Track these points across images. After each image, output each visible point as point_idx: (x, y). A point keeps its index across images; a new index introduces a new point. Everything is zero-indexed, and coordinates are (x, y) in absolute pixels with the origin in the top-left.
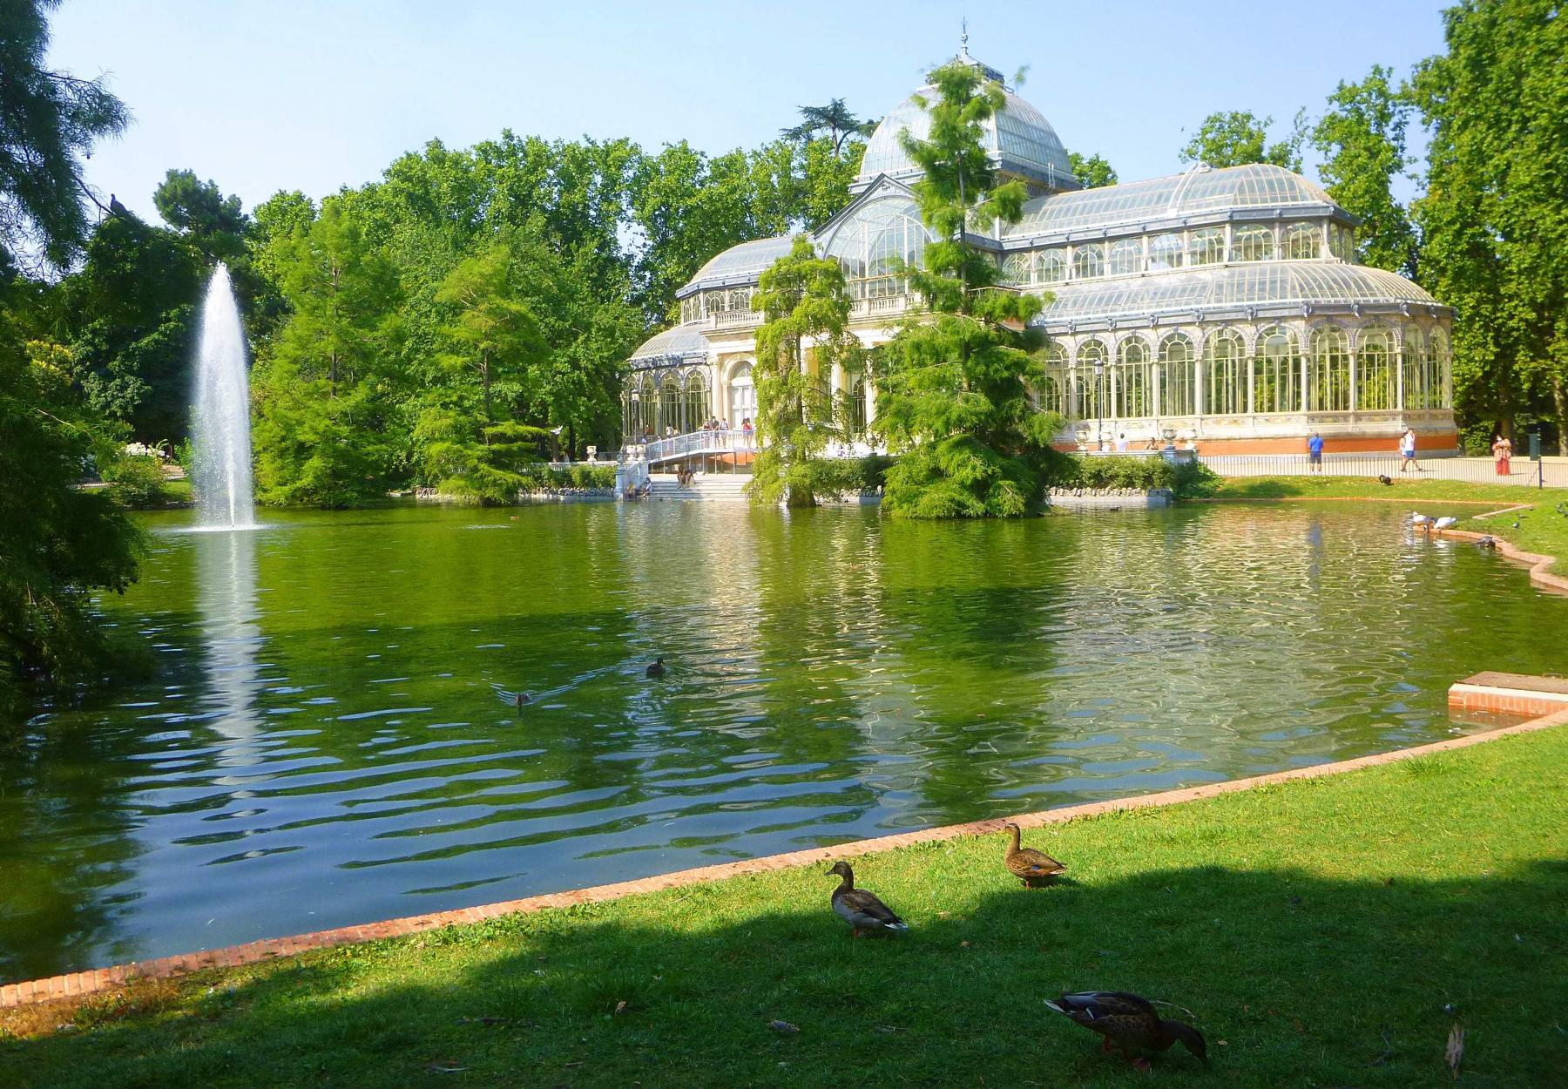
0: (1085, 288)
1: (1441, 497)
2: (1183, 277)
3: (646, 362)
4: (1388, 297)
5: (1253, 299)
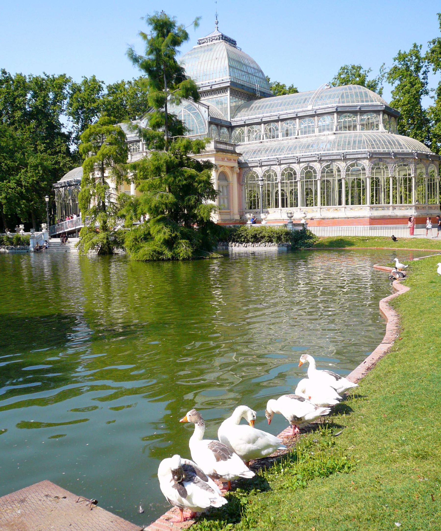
0: (269, 144)
1: (416, 247)
2: (314, 138)
3: (65, 183)
4: (409, 150)
5: (345, 149)
